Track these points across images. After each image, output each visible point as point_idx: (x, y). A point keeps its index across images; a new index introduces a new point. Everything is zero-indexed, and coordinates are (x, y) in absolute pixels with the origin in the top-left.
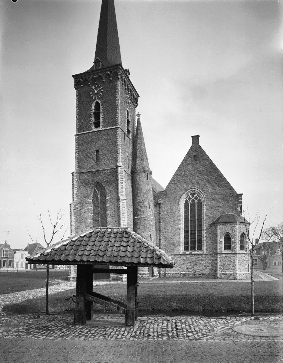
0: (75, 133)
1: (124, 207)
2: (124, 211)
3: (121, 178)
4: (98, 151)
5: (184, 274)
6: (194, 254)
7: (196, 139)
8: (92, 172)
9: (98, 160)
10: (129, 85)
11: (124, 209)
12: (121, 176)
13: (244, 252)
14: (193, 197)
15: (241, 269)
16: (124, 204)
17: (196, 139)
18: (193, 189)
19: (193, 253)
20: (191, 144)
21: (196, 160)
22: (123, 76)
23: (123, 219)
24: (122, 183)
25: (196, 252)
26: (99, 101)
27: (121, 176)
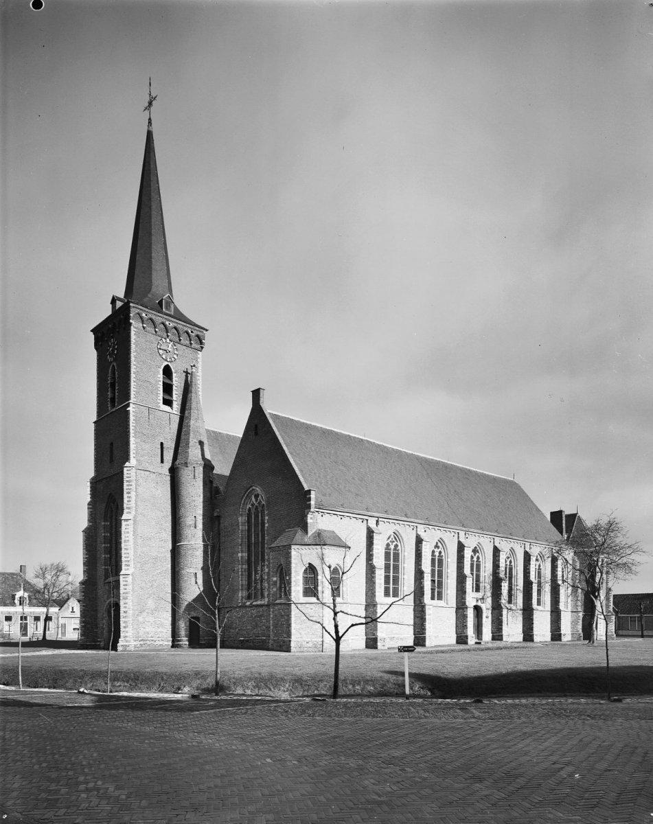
0: (95, 419)
1: (128, 532)
2: (127, 539)
3: (128, 485)
4: (112, 444)
5: (243, 640)
6: (254, 606)
7: (256, 394)
8: (106, 478)
9: (112, 461)
10: (167, 323)
11: (127, 535)
12: (127, 481)
13: (314, 600)
14: (256, 501)
15: (303, 633)
16: (127, 527)
17: (256, 394)
18: (254, 488)
19: (254, 603)
20: (251, 406)
21: (256, 434)
22: (144, 315)
23: (126, 551)
24: (128, 493)
25: (259, 603)
26: (115, 364)
27: (127, 481)
